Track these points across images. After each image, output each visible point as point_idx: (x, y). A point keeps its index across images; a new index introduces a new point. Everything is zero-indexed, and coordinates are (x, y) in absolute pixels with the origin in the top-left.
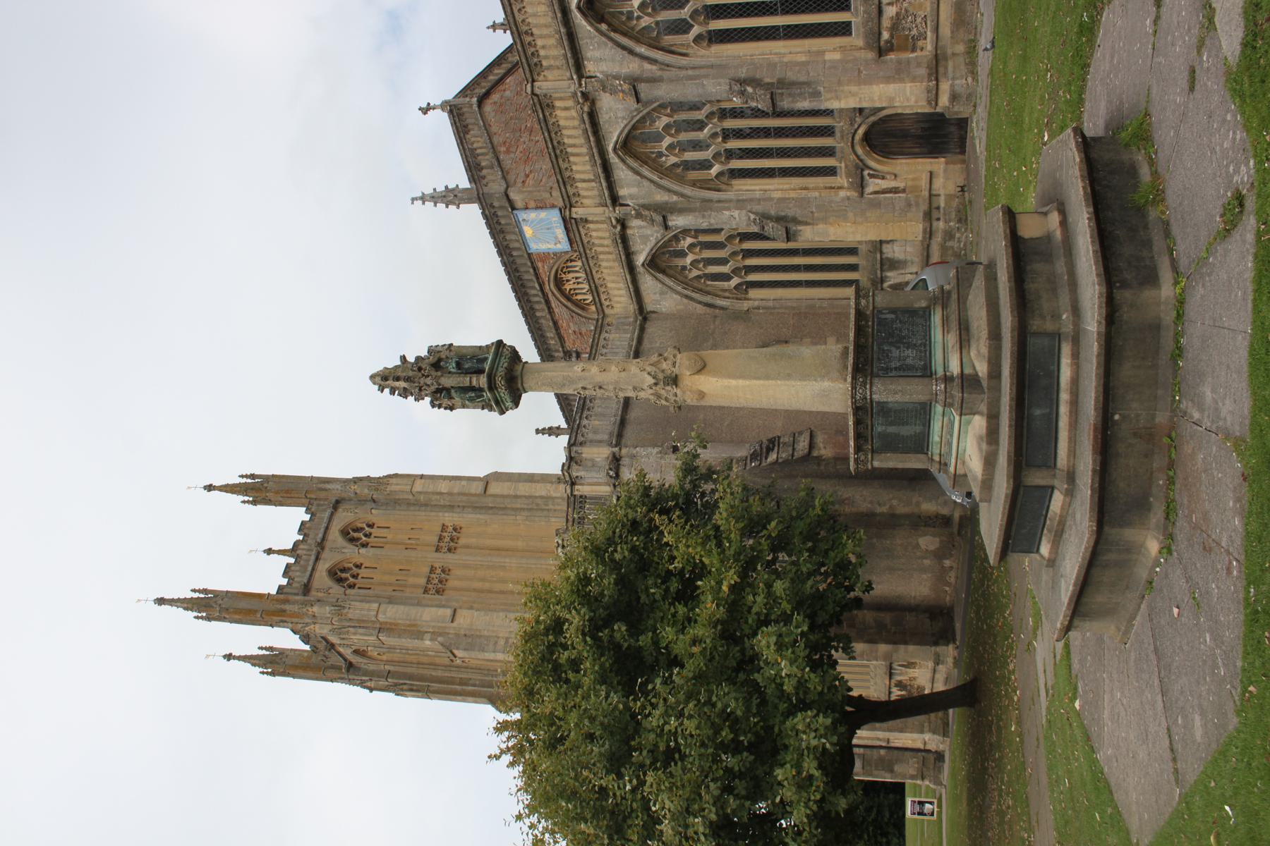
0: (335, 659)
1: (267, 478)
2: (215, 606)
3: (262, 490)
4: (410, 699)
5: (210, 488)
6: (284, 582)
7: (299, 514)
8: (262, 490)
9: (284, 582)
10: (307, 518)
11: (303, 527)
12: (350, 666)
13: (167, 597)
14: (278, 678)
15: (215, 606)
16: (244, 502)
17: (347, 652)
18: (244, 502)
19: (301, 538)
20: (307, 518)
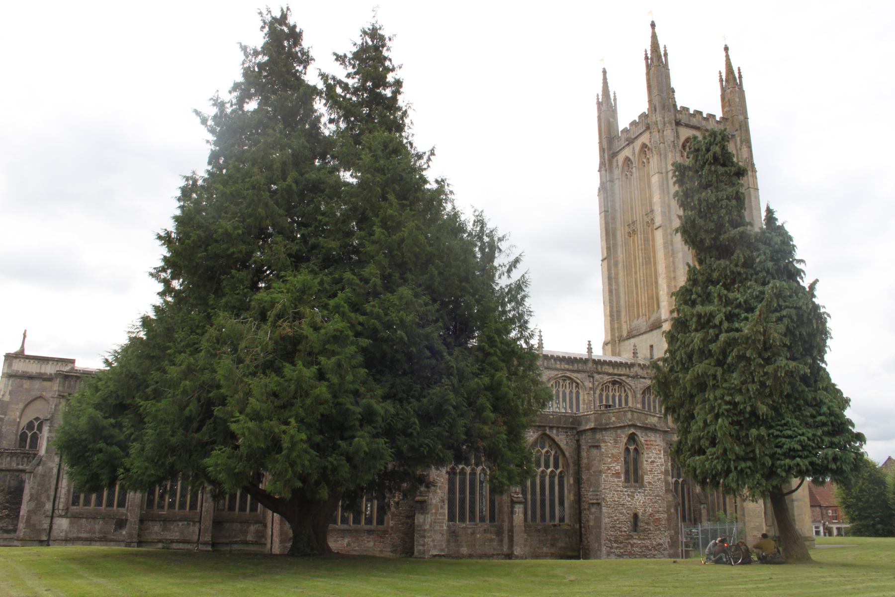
0: (618, 145)
1: (666, 66)
2: (657, 65)
3: (732, 86)
4: (597, 199)
5: (653, 25)
6: (691, 112)
7: (719, 115)
8: (732, 86)
9: (691, 112)
10: (718, 119)
11: (711, 116)
12: (614, 155)
13: (730, 53)
14: (596, 107)
15: (657, 65)
16: (720, 73)
17: (627, 152)
18: (720, 73)
19: (705, 116)
20: (718, 119)
